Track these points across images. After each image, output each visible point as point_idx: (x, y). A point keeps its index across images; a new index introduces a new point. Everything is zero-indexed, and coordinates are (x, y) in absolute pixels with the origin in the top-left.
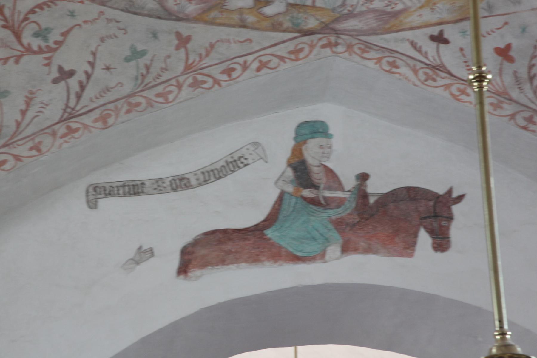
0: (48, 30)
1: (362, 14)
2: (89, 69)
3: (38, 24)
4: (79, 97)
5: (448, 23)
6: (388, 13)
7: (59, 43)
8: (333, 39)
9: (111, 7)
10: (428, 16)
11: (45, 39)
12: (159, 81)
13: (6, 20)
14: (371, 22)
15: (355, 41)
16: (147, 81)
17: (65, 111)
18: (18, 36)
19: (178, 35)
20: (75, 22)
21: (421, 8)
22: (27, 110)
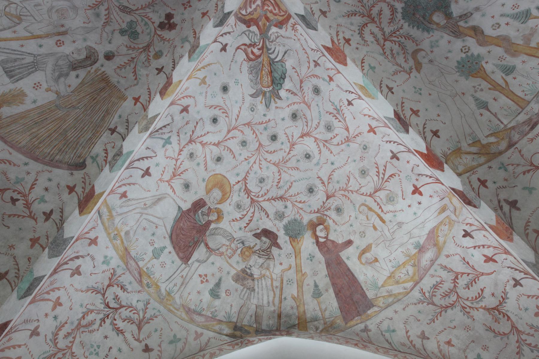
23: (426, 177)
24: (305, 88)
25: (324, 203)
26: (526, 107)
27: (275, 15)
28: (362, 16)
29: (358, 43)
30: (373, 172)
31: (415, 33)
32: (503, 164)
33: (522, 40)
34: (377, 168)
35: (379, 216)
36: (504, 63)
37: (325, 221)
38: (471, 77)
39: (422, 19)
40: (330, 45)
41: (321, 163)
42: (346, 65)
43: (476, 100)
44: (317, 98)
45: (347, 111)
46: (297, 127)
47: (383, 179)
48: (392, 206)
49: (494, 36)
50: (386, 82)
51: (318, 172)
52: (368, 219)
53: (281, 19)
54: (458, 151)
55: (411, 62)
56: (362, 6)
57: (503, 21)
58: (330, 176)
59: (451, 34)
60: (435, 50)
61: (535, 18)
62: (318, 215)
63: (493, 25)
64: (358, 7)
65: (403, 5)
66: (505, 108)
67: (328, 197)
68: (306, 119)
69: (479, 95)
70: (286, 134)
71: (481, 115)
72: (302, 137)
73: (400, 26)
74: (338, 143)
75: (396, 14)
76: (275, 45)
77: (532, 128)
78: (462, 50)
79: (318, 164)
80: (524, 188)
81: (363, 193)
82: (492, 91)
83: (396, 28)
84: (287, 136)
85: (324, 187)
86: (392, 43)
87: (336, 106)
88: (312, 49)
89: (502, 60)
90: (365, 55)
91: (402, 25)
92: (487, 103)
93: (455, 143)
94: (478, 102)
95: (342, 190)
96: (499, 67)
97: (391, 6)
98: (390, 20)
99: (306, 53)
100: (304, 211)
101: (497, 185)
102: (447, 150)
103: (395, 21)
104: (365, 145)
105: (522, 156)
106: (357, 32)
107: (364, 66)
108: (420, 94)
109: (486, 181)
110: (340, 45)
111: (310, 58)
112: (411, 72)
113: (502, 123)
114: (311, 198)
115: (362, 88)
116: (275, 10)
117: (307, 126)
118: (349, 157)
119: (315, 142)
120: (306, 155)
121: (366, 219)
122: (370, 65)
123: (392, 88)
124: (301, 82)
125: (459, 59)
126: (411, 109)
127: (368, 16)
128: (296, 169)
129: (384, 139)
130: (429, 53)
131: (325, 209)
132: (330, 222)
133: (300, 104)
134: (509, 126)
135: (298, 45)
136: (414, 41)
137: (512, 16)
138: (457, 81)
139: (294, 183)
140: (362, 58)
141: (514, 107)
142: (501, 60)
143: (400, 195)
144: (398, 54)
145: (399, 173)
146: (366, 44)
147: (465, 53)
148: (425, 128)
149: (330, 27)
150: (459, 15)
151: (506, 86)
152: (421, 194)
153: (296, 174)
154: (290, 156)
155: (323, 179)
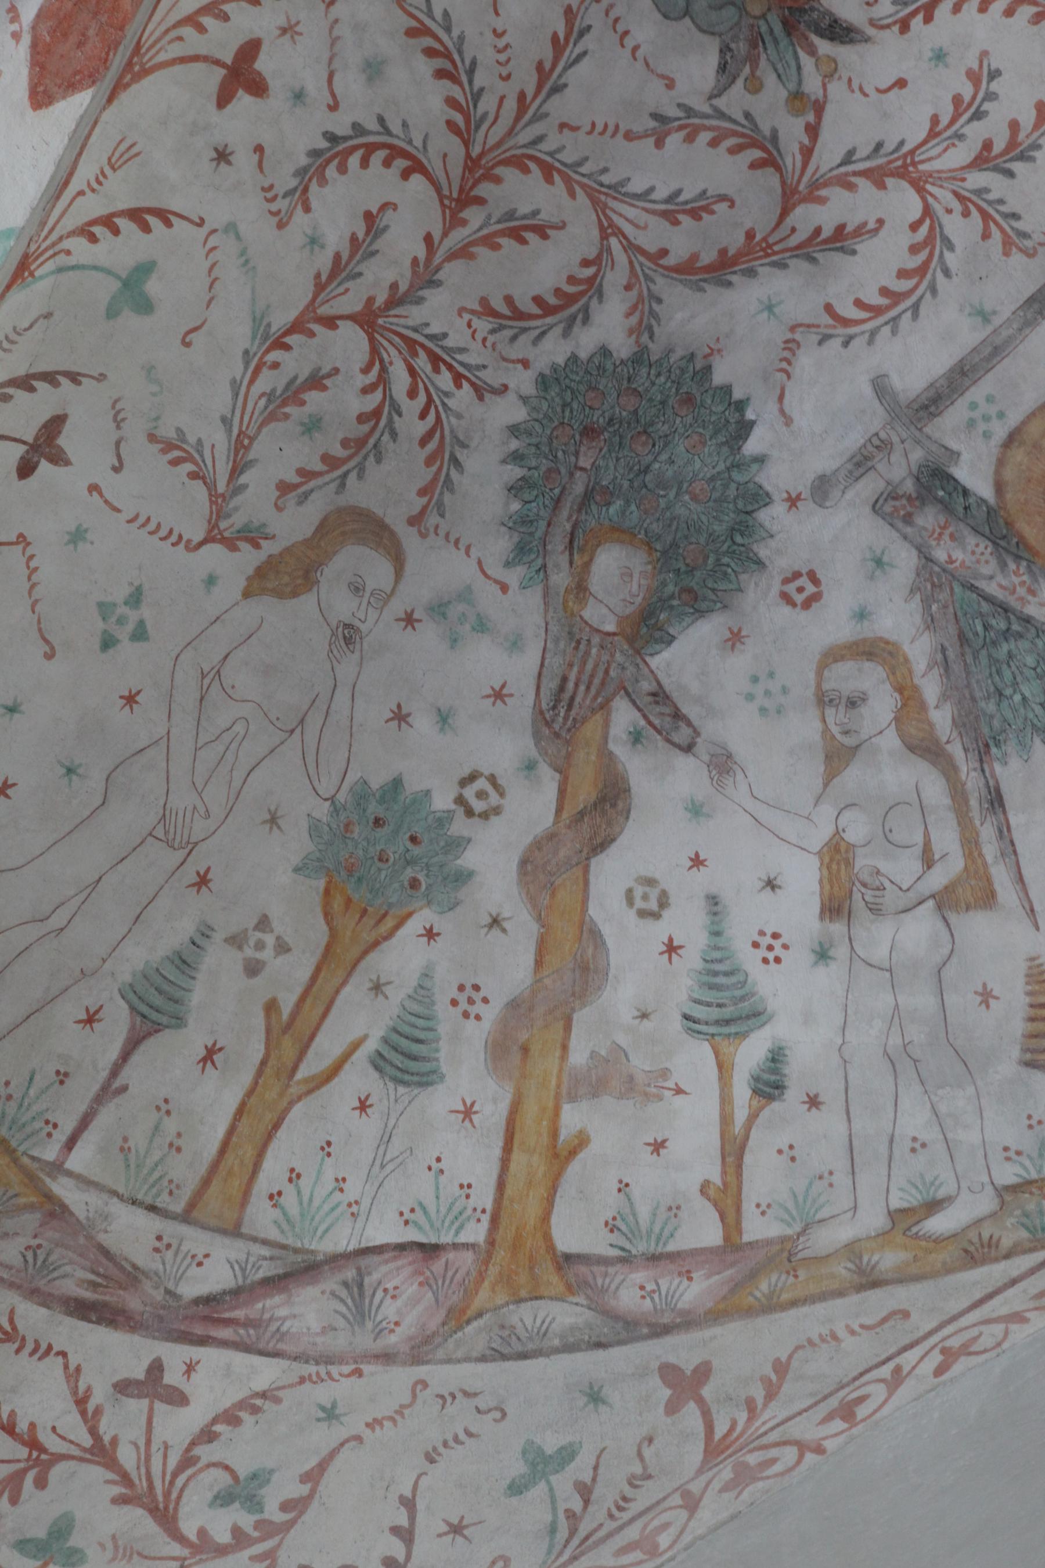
0: (260, 1478)
3: (227, 1468)
7: (296, 1506)
9: (449, 1361)
11: (253, 1503)
12: (626, 1516)
13: (126, 1479)
16: (583, 1530)
19: (669, 1373)
20: (344, 1433)
26: (204, 1227)
28: (459, 118)
29: (259, 149)
33: (593, 1054)
36: (446, 1017)
38: (322, 884)
39: (579, 488)
49: (591, 912)
56: (522, 97)
59: (550, 685)
60: (429, 633)
61: (720, 1066)
63: (650, 882)
64: (507, 78)
65: (622, 347)
66: (171, 1126)
73: (491, 377)
75: (558, 330)
78: (472, 777)
82: (259, 1021)
86: (366, 371)
89: (463, 1005)
90: (201, 223)
92: (179, 1021)
94: (171, 973)
96: (415, 1007)
97: (590, 281)
98: (504, 309)
103: (514, 338)
107: (116, 231)
108: (108, 643)
110: (187, 31)
112: (231, 544)
113: (71, 1144)
122: (145, 269)
123: (59, 458)
125: (413, 785)
127: (471, 163)
130: (397, 607)
134: (62, 1189)
137: (717, 955)
138: (273, 820)
140: (175, 204)
142: (462, 998)
144: (313, 426)
146: (282, 204)
147: (460, 800)
150: (665, 682)
151: (306, 1081)
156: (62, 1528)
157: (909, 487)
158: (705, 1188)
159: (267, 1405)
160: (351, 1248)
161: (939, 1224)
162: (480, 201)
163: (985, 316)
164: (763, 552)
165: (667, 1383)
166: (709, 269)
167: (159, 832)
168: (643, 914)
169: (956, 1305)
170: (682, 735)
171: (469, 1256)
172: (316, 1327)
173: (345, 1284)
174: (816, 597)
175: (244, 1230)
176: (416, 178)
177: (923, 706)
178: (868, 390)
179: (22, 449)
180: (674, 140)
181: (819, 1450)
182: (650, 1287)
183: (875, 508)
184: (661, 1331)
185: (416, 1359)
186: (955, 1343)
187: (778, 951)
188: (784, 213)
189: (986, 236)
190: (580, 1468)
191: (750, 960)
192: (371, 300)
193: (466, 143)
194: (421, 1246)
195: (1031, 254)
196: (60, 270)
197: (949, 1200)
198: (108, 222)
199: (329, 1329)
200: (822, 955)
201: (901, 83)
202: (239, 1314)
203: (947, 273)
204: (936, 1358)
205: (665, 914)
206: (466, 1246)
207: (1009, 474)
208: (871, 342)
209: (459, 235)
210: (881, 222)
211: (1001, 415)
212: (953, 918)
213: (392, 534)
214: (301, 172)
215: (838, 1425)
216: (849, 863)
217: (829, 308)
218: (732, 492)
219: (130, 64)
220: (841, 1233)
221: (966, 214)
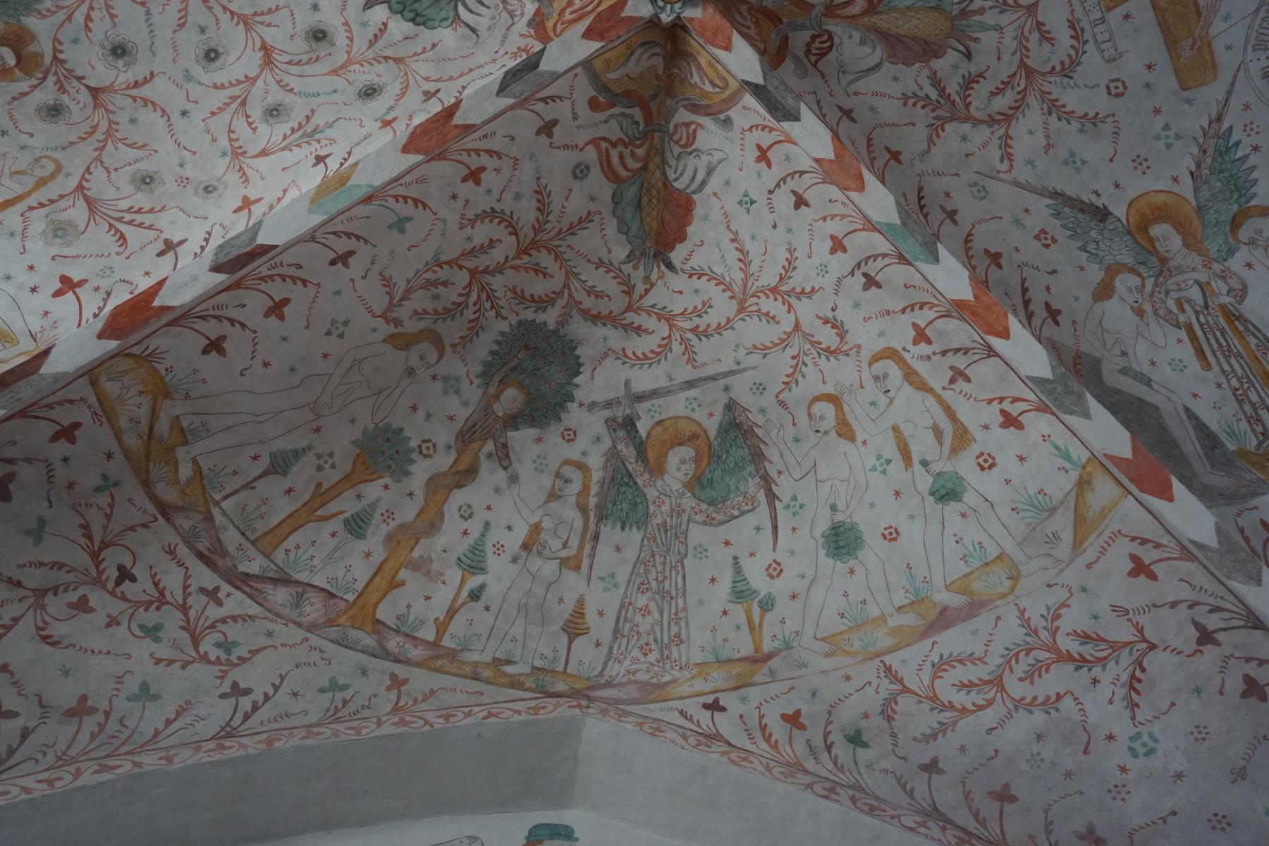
0: (235, 644)
1: (622, 684)
2: (271, 692)
3: (225, 635)
4: (247, 717)
5: (723, 691)
6: (653, 685)
8: (584, 703)
9: (319, 636)
10: (700, 685)
12: (355, 717)
13: (188, 622)
14: (633, 692)
15: (609, 708)
16: (339, 714)
17: (223, 729)
18: (196, 642)
19: (393, 676)
20: (270, 642)
21: (693, 678)
22: (175, 719)
23: (99, 307)
24: (381, 68)
25: (80, 79)
26: (258, 549)
27: (561, 13)
29: (467, 201)
30: (142, 200)
31: (483, 347)
32: (116, 484)
33: (421, 556)
34: (151, 210)
35: (20, 198)
36: (377, 518)
37: (28, 73)
39: (514, 364)
40: (458, 120)
41: (191, 86)
42: (405, 150)
43: (297, 454)
44: (352, 91)
45: (306, 153)
46: (292, 37)
47: (119, 220)
48: (40, 231)
49: (445, 507)
50: (364, 253)
51: (168, 75)
52: (18, 173)
53: (549, 25)
54: (161, 390)
55: (412, 326)
56: (561, 230)
57: (475, 527)
58: (153, 103)
59: (470, 423)
60: (439, 385)
62: (48, 60)
63: (469, 507)
65: (552, 326)
66: (264, 509)
67: (94, 92)
68: (307, 63)
69: (309, 459)
70: (277, 8)
71: (255, 458)
72: (264, 47)
74: (234, 132)
75: (533, 309)
76: (496, 7)
77: (201, 556)
78: (428, 441)
79: (188, 77)
80: (42, 522)
81: (90, 173)
82: (312, 488)
83: (501, 303)
84: (270, 12)
85: (124, 86)
86: (463, 289)
87: (322, 131)
88: (464, 88)
89: (385, 517)
90: (435, 214)
91: (506, 319)
93: (186, 386)
95: (110, 127)
96: (367, 509)
97: (552, 299)
99: (462, 75)
100: (62, 25)
101: (58, 465)
102: (167, 364)
104: (215, 189)
105: (132, 529)
106: (498, 207)
107: (406, 203)
108: (328, 333)
109: (72, 441)
110: (464, 154)
111: (448, 83)
112: (388, 322)
113: (226, 497)
114: (98, 48)
115: (341, 180)
116: (572, 13)
117: (290, 63)
118: (195, 153)
119: (246, 77)
120: (216, 51)
121: (13, 169)
122: (408, 219)
123: (346, 265)
124: (398, 61)
125: (407, 434)
126: (286, 301)
127: (533, 242)
128: (183, 21)
129: (217, 229)
130: (432, 371)
131: (62, 78)
132: (23, 86)
133: (347, 52)
134: (216, 512)
135: (482, 60)
136: (466, 340)
138: (353, 421)
139: (142, 10)
140: (430, 204)
141: (261, 527)
143: (66, 252)
144: (436, 297)
145: (127, 253)
146: (465, 222)
147: (420, 447)
148: (233, 325)
149: (512, 138)
151: (318, 516)
152: (58, 294)
153: (166, 19)
154: (218, 10)
155: (147, 87)
156: (158, 627)
157: (620, 420)
158: (436, 620)
159: (249, 621)
160: (306, 581)
161: (508, 669)
162: (530, 255)
163: (671, 379)
164: (563, 416)
165: (391, 679)
166: (591, 315)
167: (312, 406)
168: (461, 516)
169: (500, 699)
170: (505, 463)
171: (344, 604)
172: (279, 602)
173: (297, 593)
174: (572, 440)
175: (272, 557)
176: (513, 237)
177: (588, 494)
178: (623, 382)
179: (335, 255)
180: (602, 270)
181: (432, 726)
182: (401, 644)
183: (606, 421)
184: (397, 661)
185: (309, 630)
186: (494, 711)
187: (500, 552)
188: (625, 312)
189: (684, 354)
190: (347, 694)
191: (489, 549)
192: (477, 267)
193: (535, 235)
194: (329, 593)
195: (694, 367)
196: (381, 205)
197: (515, 663)
198: (405, 198)
199: (283, 605)
200: (514, 560)
201: (681, 293)
202: (255, 585)
203: (666, 359)
204: (485, 713)
205: (470, 520)
206: (345, 600)
207: (653, 433)
208: (631, 367)
209: (518, 262)
210: (653, 331)
211: (660, 413)
212: (563, 569)
213: (444, 347)
214: (477, 215)
215: (442, 720)
216: (538, 534)
217: (624, 349)
218: (563, 391)
219: (440, 154)
220: (475, 657)
221: (681, 344)
